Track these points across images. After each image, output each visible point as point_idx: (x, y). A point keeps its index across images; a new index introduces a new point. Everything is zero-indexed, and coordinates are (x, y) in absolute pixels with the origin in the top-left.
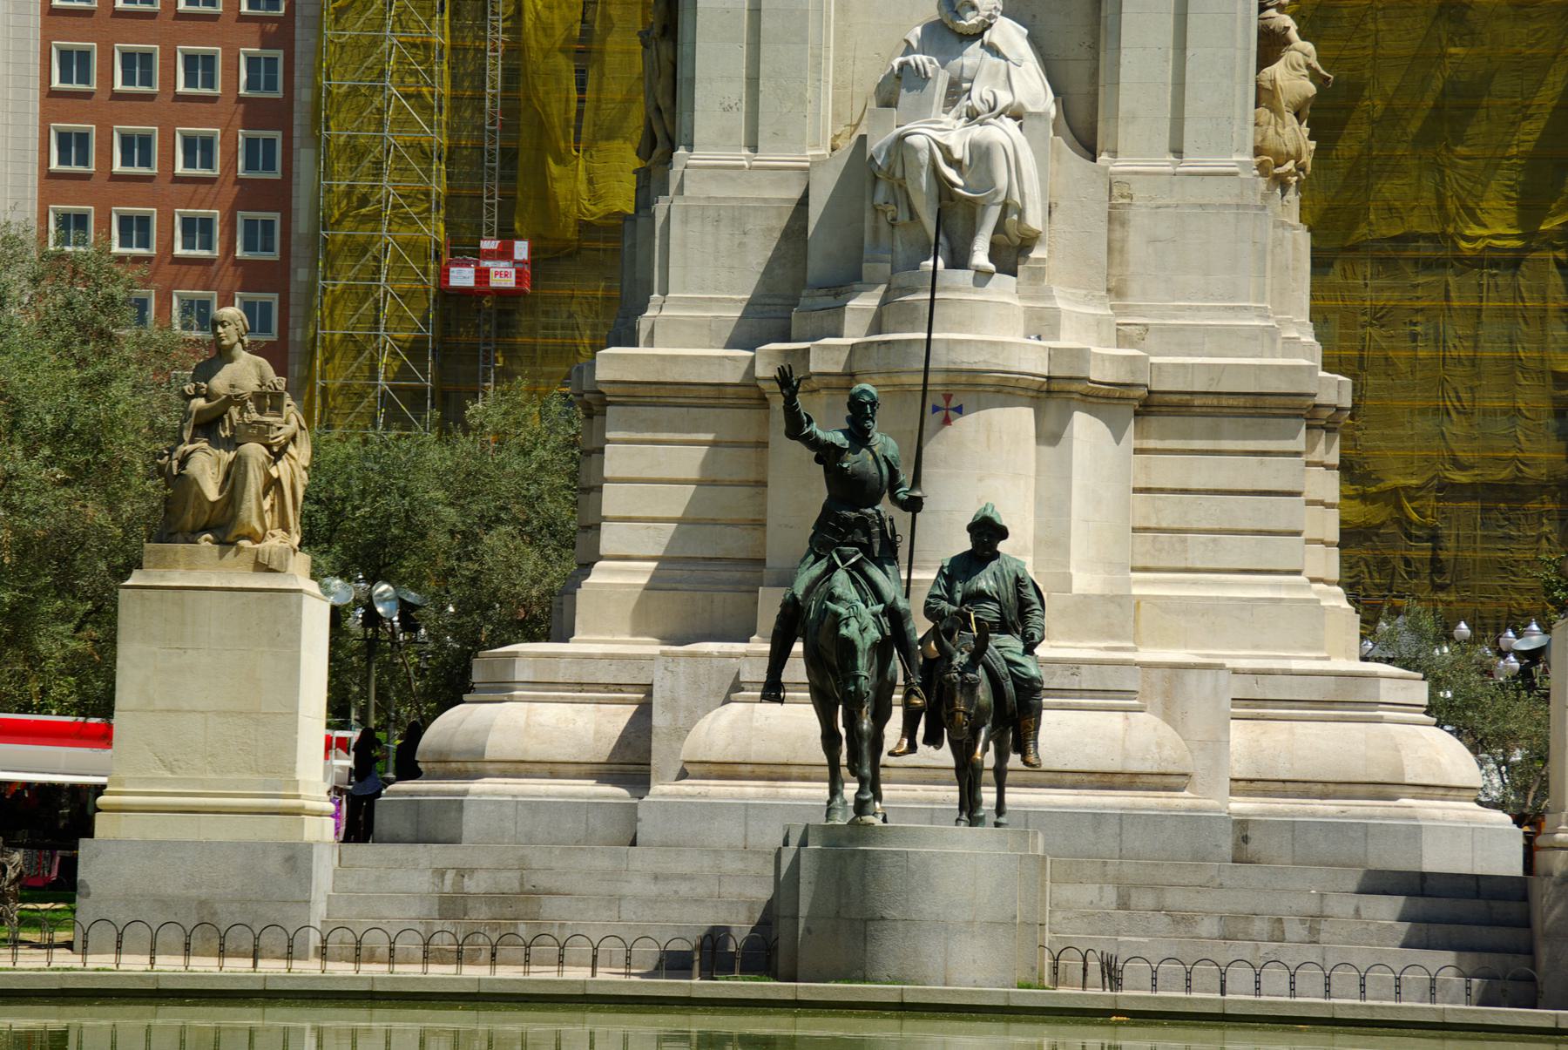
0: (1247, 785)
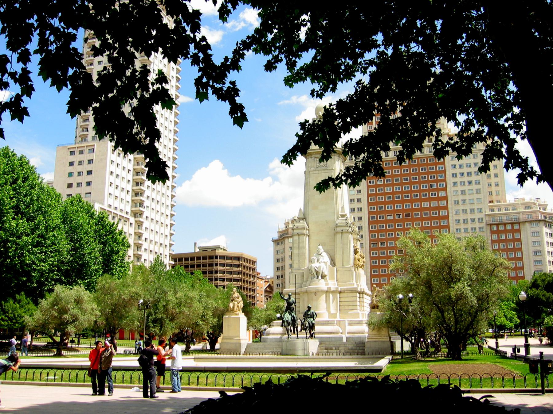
0: (348, 333)
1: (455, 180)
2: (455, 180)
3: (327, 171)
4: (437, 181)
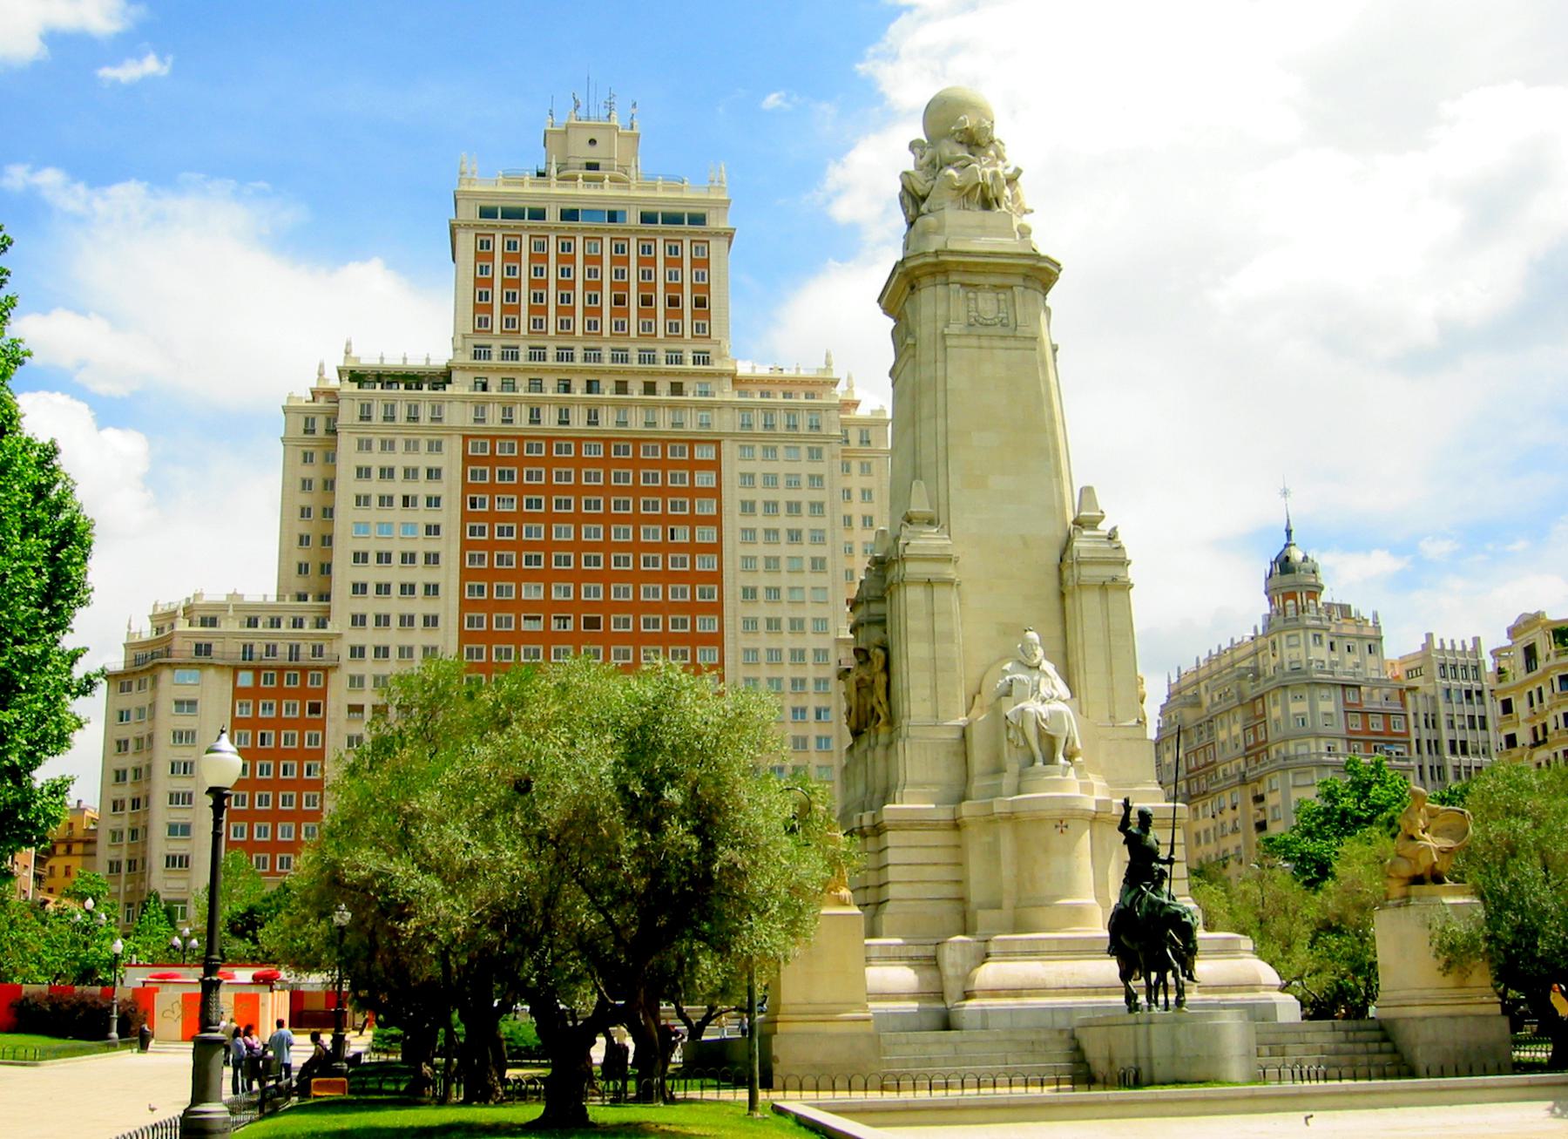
1: (748, 522)
2: (748, 522)
3: (1012, 343)
4: (694, 521)
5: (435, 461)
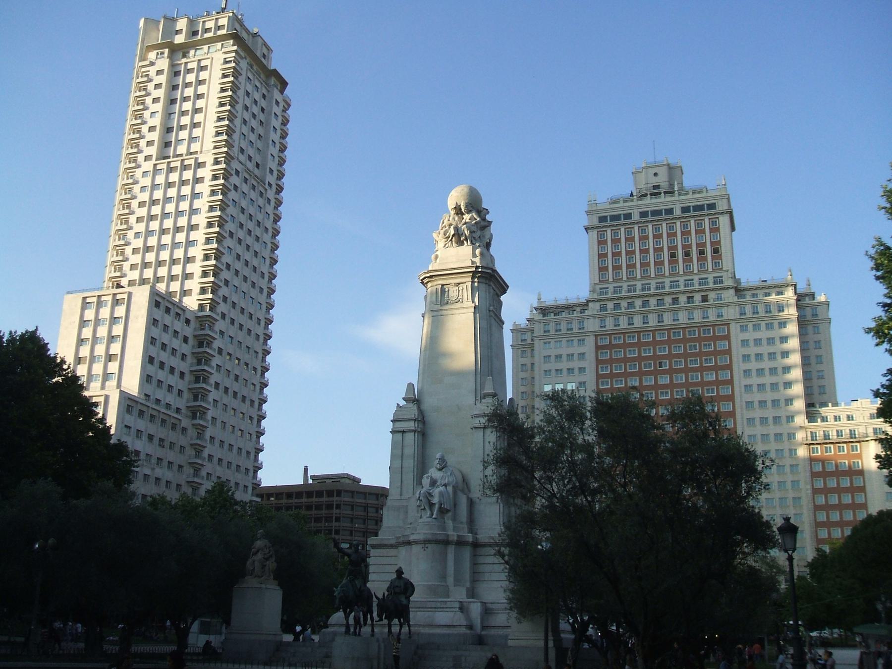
1: (747, 366)
5: (581, 350)
